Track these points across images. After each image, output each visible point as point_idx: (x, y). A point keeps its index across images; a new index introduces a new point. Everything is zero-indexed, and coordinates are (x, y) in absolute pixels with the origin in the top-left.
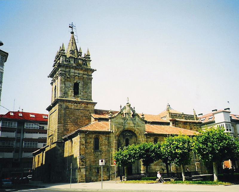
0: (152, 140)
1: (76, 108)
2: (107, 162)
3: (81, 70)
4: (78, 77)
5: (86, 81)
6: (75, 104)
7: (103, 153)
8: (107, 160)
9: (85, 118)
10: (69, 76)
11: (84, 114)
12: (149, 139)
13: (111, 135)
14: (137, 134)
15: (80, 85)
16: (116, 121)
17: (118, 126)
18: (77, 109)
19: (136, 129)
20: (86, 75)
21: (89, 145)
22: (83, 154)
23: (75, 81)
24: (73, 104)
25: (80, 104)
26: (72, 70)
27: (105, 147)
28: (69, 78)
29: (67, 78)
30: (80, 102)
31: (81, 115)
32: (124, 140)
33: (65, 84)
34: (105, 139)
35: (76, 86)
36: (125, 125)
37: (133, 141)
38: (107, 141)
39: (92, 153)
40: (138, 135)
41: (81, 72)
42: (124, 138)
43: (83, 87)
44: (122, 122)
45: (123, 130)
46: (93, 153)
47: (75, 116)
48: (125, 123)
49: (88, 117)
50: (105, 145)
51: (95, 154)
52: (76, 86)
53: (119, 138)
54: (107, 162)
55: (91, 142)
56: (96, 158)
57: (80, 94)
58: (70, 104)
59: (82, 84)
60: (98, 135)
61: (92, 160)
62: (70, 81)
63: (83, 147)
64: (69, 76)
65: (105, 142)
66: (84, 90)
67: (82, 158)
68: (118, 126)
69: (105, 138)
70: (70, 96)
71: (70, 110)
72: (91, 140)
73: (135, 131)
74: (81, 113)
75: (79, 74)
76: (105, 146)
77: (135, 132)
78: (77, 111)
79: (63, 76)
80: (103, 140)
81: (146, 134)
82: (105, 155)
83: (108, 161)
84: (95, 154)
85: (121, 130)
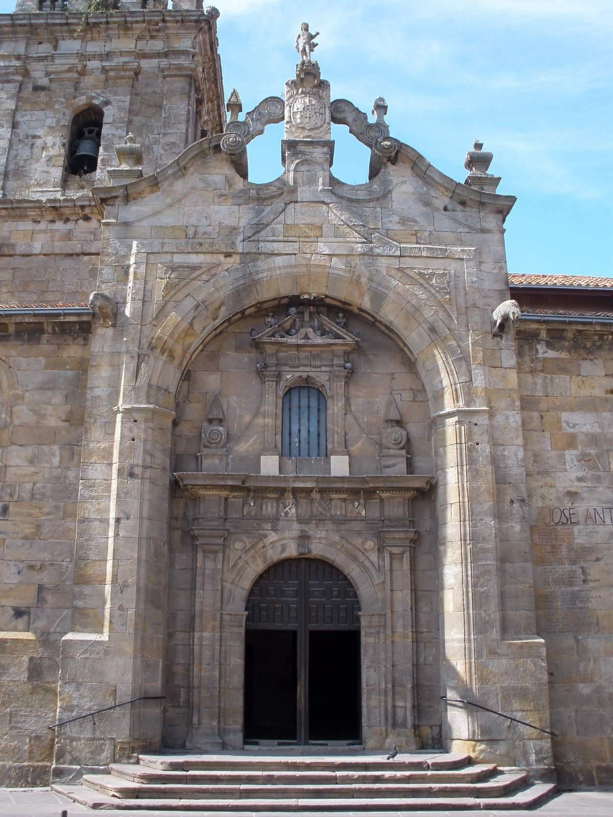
0: (598, 392)
1: (59, 246)
2: (40, 599)
3: (126, 36)
4: (103, 77)
5: (150, 90)
6: (59, 225)
8: (45, 578)
10: (47, 79)
12: (566, 386)
13: (103, 339)
14: (404, 333)
15: (109, 114)
16: (169, 219)
18: (71, 255)
20: (158, 55)
23: (82, 101)
24: (43, 225)
25: (87, 218)
26: (71, 46)
27: (31, 462)
28: (43, 88)
29: (37, 88)
30: (83, 207)
32: (262, 395)
33: (14, 125)
34: (42, 388)
35: (86, 127)
36: (266, 247)
37: (381, 400)
38: (58, 399)
40: (415, 337)
41: (127, 44)
42: (261, 374)
43: (130, 122)
44: (230, 222)
45: (238, 294)
48: (259, 227)
50: (41, 436)
53: (211, 381)
54: (40, 599)
58: (26, 226)
59: (120, 109)
62: (49, 105)
64: (44, 81)
65: (35, 412)
68: (178, 259)
69: (40, 378)
70: (39, 185)
71: (17, 262)
73: (378, 298)
75: (108, 55)
76: (29, 451)
77: (389, 314)
78: (68, 262)
79: (8, 82)
80: (19, 398)
81: (506, 318)
82: (28, 530)
83: (57, 589)
85: (218, 287)
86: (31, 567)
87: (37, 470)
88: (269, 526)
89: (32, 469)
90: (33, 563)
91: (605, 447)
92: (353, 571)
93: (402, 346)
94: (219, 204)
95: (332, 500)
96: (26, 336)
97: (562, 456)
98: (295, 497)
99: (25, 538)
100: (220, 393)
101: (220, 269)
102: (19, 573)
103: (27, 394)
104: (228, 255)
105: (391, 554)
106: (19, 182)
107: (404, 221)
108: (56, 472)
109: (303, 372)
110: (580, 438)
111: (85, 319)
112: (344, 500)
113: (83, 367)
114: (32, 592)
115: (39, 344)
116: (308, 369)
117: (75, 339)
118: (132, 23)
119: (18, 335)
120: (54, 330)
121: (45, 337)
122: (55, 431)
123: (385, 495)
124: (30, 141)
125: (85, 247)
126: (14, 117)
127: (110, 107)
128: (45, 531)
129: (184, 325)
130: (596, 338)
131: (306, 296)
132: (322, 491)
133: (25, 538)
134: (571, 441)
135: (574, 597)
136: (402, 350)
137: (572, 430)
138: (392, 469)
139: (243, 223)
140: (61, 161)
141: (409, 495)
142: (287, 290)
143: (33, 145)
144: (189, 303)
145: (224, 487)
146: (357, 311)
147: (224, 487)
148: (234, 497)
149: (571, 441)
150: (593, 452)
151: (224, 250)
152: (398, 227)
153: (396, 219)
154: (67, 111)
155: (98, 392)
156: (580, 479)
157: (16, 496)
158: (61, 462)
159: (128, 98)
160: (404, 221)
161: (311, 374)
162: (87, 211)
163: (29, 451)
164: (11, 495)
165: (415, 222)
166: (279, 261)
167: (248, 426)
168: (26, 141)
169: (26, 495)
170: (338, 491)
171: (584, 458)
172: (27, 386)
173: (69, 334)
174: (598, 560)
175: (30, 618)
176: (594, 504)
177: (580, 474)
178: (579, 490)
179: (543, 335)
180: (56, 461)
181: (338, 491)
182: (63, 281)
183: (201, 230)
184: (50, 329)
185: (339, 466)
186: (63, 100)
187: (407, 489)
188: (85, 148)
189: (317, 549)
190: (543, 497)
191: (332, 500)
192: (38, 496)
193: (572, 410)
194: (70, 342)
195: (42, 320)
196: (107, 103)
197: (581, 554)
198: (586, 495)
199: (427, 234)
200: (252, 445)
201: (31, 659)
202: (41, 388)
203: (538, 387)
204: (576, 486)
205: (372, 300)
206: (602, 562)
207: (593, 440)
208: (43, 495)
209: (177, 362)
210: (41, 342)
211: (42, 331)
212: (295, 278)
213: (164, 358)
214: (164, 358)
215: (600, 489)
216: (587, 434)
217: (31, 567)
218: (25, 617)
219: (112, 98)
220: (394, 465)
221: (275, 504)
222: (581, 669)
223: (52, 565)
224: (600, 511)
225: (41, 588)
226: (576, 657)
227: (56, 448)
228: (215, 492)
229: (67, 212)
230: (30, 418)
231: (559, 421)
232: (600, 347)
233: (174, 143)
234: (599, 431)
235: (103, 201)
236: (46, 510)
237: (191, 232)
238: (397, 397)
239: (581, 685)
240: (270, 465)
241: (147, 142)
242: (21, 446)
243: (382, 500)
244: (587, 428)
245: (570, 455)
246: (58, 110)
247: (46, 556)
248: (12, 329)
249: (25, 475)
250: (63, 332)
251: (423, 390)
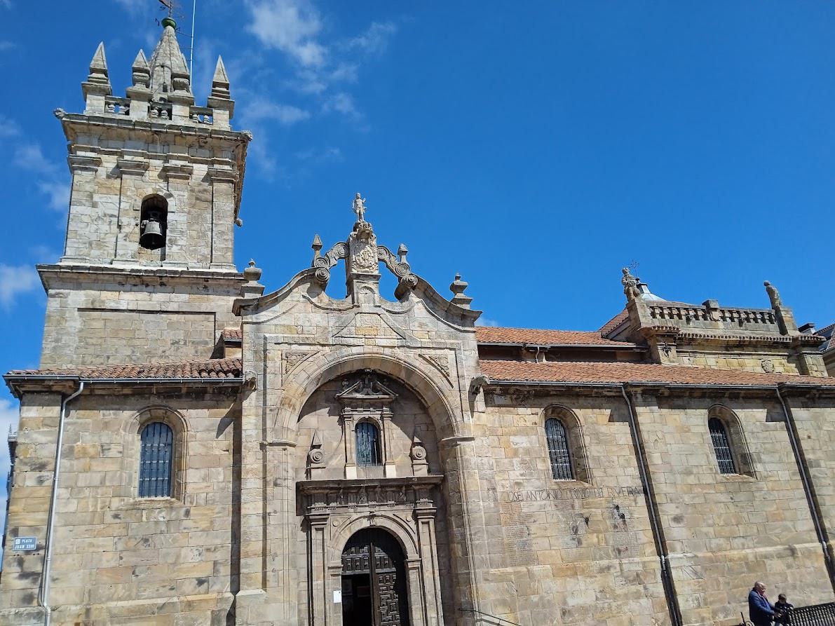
2: (215, 571)
7: (187, 513)
9: (193, 351)
11: (187, 334)
16: (285, 320)
17: (295, 347)
19: (417, 364)
21: (87, 470)
22: (35, 529)
31: (170, 336)
39: (109, 518)
44: (324, 324)
46: (116, 516)
47: (137, 342)
49: (206, 343)
51: (134, 525)
52: (154, 208)
54: (215, 571)
55: (104, 449)
56: (135, 550)
57: (173, 242)
60: (157, 407)
61: (109, 560)
63: (40, 481)
66: (195, 227)
67: (28, 552)
72: (105, 440)
74: (170, 325)
76: (203, 472)
79: (86, 169)
82: (204, 524)
84: (127, 526)
86: (208, 550)
87: (209, 484)
88: (352, 510)
89: (205, 484)
90: (210, 547)
91: (534, 455)
92: (401, 534)
93: (420, 398)
94: (315, 312)
95: (387, 492)
96: (194, 396)
97: (511, 462)
98: (366, 491)
99: (203, 530)
100: (318, 428)
101: (319, 354)
102: (200, 554)
103: (198, 434)
104: (323, 345)
105: (423, 523)
106: (102, 251)
107: (421, 325)
108: (221, 485)
109: (366, 415)
110: (521, 450)
111: (237, 385)
112: (393, 491)
113: (235, 418)
114: (211, 564)
115: (203, 400)
116: (369, 413)
117: (228, 397)
118: (186, 135)
119: (188, 394)
120: (214, 391)
121: (207, 396)
122: (219, 458)
123: (417, 488)
124: (107, 219)
125: (163, 307)
126: (91, 197)
127: (172, 198)
128: (216, 525)
129: (301, 389)
130: (526, 393)
131: (368, 370)
132: (382, 487)
133: (203, 530)
134: (516, 453)
135: (525, 544)
136: (420, 400)
137: (516, 446)
138: (419, 472)
139: (331, 324)
140: (137, 237)
141: (430, 486)
142: (357, 367)
143: (111, 222)
144: (304, 375)
145: (327, 488)
146: (394, 378)
147: (327, 488)
148: (331, 493)
149: (516, 453)
150: (527, 459)
151: (322, 343)
152: (419, 329)
153: (417, 324)
154: (137, 198)
155: (249, 432)
156: (522, 475)
157: (194, 504)
158: (224, 478)
159: (186, 194)
160: (421, 325)
161: (371, 416)
162: (164, 280)
163: (203, 472)
164: (191, 503)
165: (427, 325)
166: (355, 350)
167: (336, 449)
168: (105, 218)
169: (202, 502)
170: (391, 486)
171: (523, 462)
172: (197, 429)
173: (224, 394)
174: (535, 521)
175: (209, 585)
176: (531, 489)
177: (522, 472)
178: (522, 481)
179: (498, 391)
180: (221, 478)
181: (391, 486)
182: (147, 331)
183: (305, 329)
184: (211, 391)
185: (392, 472)
186: (134, 189)
187: (430, 484)
188: (155, 228)
189: (379, 522)
190: (503, 486)
191: (387, 492)
192: (210, 502)
193: (515, 435)
194: (226, 399)
195: (208, 386)
196: (171, 195)
197: (526, 519)
198: (525, 484)
199: (434, 333)
200: (339, 461)
201: (213, 612)
202: (208, 430)
203: (496, 422)
204: (520, 479)
205: (406, 373)
206: (537, 522)
207: (528, 452)
208: (214, 500)
209: (297, 412)
210: (205, 399)
211: (206, 392)
212: (363, 360)
213: (291, 410)
214: (291, 410)
215: (533, 480)
216: (524, 448)
217: (208, 550)
218: (206, 584)
219: (173, 192)
220: (420, 469)
221: (355, 496)
222: (532, 586)
223: (222, 547)
224: (533, 492)
225: (215, 563)
226: (529, 579)
227: (220, 469)
228: (321, 491)
229: (149, 279)
230: (202, 450)
231: (508, 441)
232: (528, 398)
233: (223, 232)
234: (529, 445)
235: (242, 307)
236: (216, 511)
237: (300, 329)
238: (418, 428)
239: (532, 596)
240: (352, 474)
241: (203, 229)
242: (197, 469)
243: (415, 490)
244: (524, 445)
245: (516, 461)
246: (130, 196)
247: (218, 541)
248: (184, 391)
249: (201, 489)
250: (220, 393)
251: (432, 423)
